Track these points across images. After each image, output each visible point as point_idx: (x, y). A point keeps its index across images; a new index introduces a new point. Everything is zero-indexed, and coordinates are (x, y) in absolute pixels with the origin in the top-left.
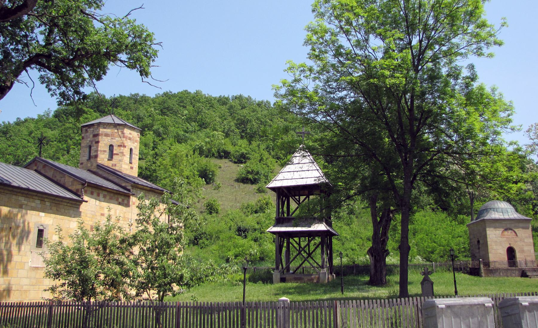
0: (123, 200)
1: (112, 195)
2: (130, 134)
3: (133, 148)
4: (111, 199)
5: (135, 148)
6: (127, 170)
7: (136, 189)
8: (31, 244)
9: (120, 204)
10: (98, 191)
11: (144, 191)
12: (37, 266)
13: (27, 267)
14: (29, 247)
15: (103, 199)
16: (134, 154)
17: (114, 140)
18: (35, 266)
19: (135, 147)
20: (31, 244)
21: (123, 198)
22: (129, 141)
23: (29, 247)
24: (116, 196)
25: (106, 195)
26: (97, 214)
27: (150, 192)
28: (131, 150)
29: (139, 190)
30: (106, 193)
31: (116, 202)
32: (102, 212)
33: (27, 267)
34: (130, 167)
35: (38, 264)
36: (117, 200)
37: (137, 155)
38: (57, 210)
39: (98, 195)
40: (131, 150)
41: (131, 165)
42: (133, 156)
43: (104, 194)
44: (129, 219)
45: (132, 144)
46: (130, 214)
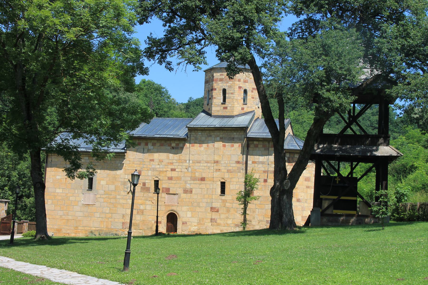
0: (177, 145)
1: (163, 142)
2: (221, 75)
3: (226, 88)
4: (162, 145)
5: (230, 87)
6: (218, 111)
7: (196, 131)
8: (83, 189)
9: (173, 148)
10: (146, 142)
11: (208, 132)
12: (88, 203)
13: (80, 204)
14: (81, 190)
15: (152, 147)
16: (228, 93)
17: (210, 86)
18: (86, 203)
19: (228, 86)
20: (83, 189)
21: (176, 142)
22: (220, 82)
23: (81, 190)
24: (169, 142)
25: (155, 143)
26: (145, 160)
27: (216, 131)
28: (224, 91)
29: (199, 131)
30: (155, 141)
31: (169, 148)
32: (151, 158)
33: (80, 204)
34: (222, 108)
35: (89, 202)
36: (170, 145)
37: (232, 94)
38: (103, 162)
39: (147, 144)
40: (224, 91)
41: (224, 106)
42: (227, 95)
43: (153, 143)
44: (186, 161)
45: (225, 84)
46: (188, 156)
